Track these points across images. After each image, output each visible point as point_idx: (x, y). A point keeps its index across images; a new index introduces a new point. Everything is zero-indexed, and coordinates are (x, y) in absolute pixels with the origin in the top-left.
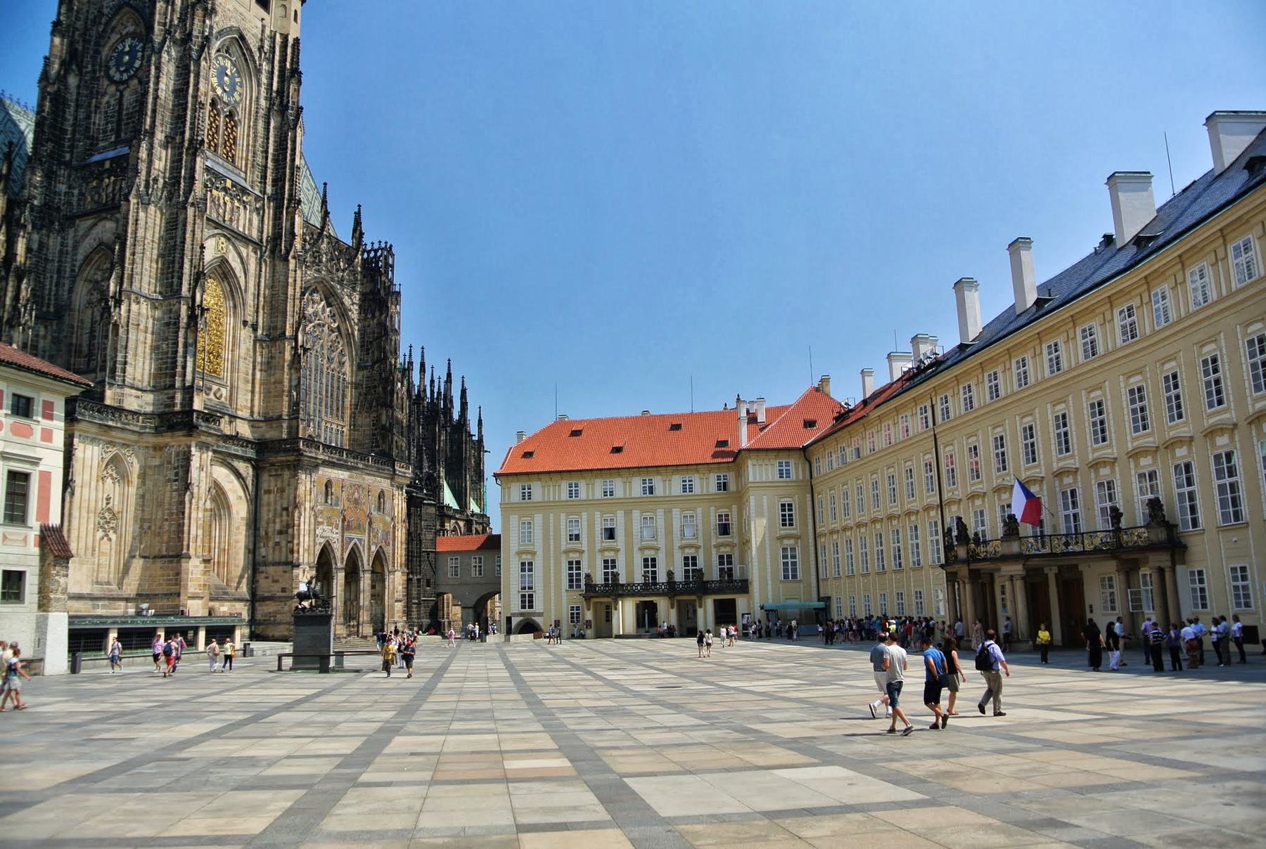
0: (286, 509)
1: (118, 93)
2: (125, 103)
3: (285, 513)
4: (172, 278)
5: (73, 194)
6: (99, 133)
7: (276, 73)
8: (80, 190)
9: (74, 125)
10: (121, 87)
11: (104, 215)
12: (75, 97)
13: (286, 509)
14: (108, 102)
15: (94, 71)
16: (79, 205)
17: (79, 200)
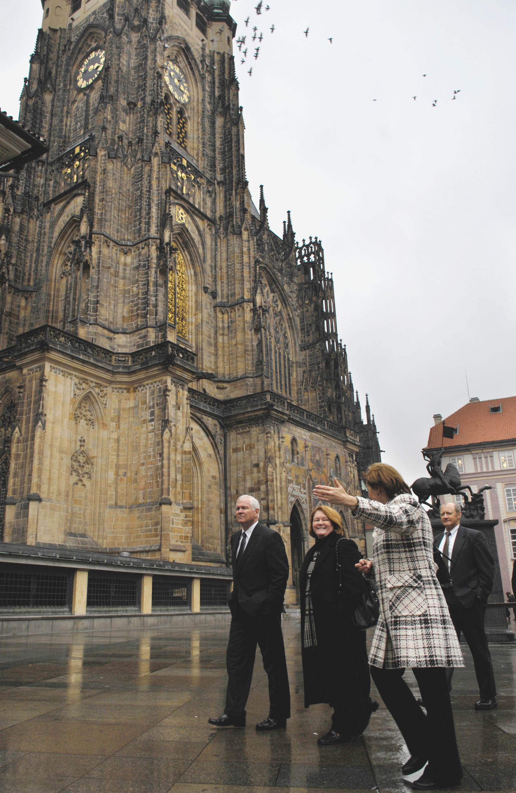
0: (257, 465)
1: (85, 97)
2: (91, 101)
3: (255, 470)
4: (140, 223)
5: (49, 185)
6: (70, 133)
7: (217, 84)
8: (55, 179)
9: (50, 130)
10: (87, 92)
11: (76, 192)
12: (50, 109)
13: (257, 465)
14: (77, 107)
15: (65, 86)
16: (54, 191)
17: (55, 187)
